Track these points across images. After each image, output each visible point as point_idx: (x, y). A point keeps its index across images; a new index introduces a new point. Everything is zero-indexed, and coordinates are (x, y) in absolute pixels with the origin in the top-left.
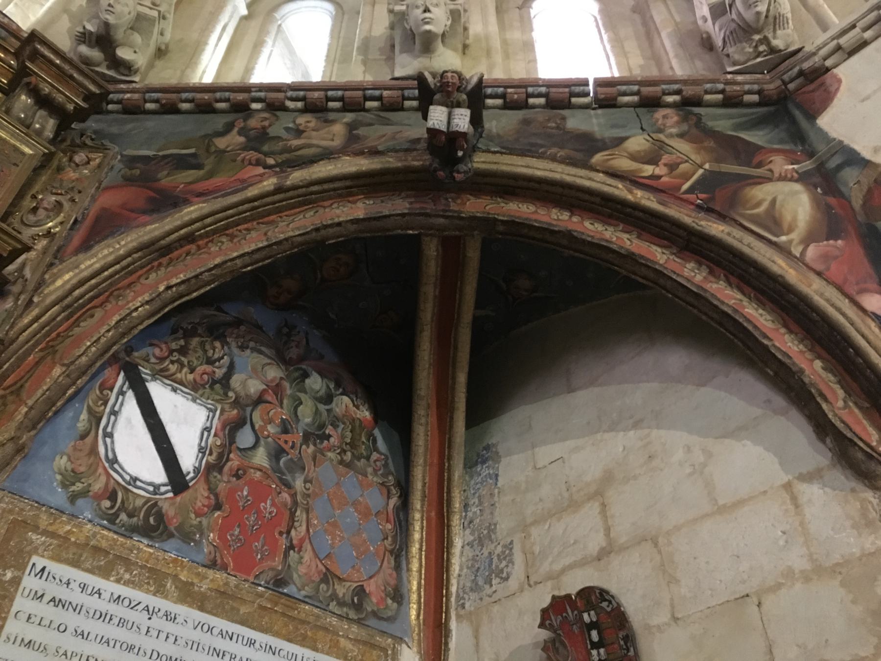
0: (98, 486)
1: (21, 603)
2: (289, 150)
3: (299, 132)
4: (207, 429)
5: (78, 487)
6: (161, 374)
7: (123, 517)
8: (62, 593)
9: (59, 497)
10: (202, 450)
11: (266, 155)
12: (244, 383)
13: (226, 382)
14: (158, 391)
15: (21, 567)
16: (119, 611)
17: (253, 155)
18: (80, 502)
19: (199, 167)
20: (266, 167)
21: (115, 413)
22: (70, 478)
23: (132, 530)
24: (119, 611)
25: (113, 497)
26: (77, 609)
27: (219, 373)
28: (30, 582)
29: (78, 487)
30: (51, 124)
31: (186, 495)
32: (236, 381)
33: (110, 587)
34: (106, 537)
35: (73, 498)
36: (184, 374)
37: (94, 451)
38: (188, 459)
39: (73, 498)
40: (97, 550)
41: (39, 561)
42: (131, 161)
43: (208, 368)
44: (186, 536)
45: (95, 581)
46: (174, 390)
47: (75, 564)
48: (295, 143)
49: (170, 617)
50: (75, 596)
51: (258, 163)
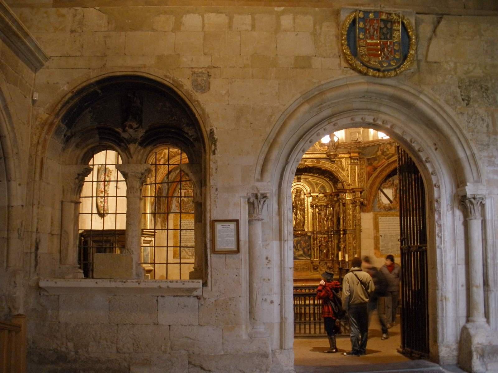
0: (382, 207)
1: (380, 223)
2: (387, 155)
3: (388, 149)
4: (393, 193)
5: (380, 208)
6: (384, 188)
7: (386, 209)
8: (383, 220)
9: (378, 210)
10: (393, 196)
11: (385, 156)
12: (396, 182)
13: (393, 184)
14: (385, 190)
15: (378, 219)
16: (390, 220)
17: (383, 157)
18: (381, 209)
19: (377, 160)
20: (386, 159)
21: (380, 196)
22: (379, 207)
23: (388, 210)
24: (390, 220)
25: (384, 207)
26: (385, 221)
27: (392, 182)
28: (379, 220)
29: (380, 208)
30: (357, 160)
31: (393, 203)
32: (395, 183)
33: (388, 218)
34: (385, 212)
35: (380, 209)
36: (387, 186)
37: (380, 203)
38: (391, 198)
39: (380, 209)
40: (385, 214)
41: (380, 218)
42: (368, 159)
43: (390, 183)
44: (394, 208)
45: (386, 218)
46: (386, 189)
47: (383, 216)
48: (388, 152)
49: (395, 219)
50: (385, 220)
51: (384, 159)
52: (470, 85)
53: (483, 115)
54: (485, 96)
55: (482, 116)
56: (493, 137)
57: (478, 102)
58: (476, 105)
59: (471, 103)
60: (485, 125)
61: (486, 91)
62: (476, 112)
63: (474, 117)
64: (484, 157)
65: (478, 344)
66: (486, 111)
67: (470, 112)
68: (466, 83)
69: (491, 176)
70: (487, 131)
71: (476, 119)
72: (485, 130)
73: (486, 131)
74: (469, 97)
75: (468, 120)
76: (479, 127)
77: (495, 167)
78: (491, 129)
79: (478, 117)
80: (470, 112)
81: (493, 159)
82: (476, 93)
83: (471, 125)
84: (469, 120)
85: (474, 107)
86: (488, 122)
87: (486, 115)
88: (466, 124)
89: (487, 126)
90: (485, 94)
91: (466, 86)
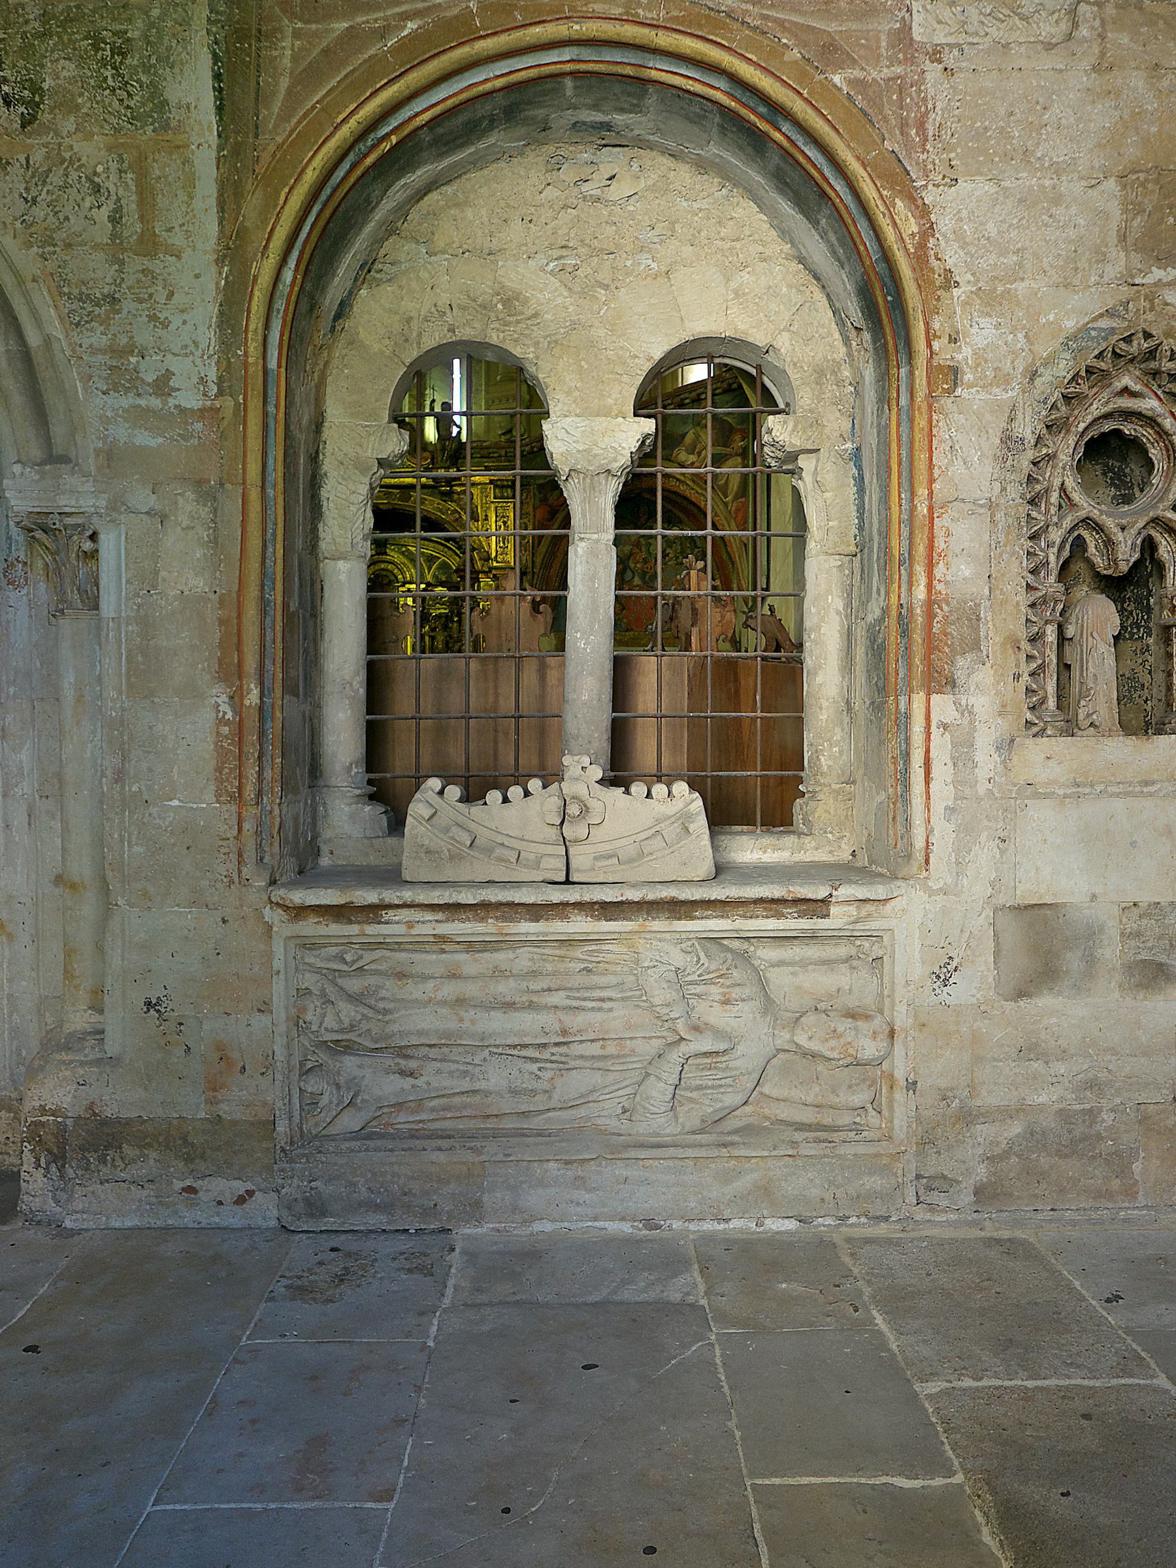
52: (44, 35)
53: (100, 169)
54: (110, 82)
55: (95, 174)
56: (134, 264)
57: (78, 107)
58: (69, 124)
59: (45, 117)
60: (105, 212)
61: (118, 59)
62: (67, 155)
63: (56, 179)
64: (93, 350)
65: (43, 1110)
66: (110, 149)
67: (38, 157)
68: (27, 22)
69: (121, 433)
70: (114, 236)
71: (64, 187)
72: (102, 231)
73: (106, 240)
74: (36, 89)
75: (27, 189)
76: (76, 223)
77: (139, 395)
78: (133, 226)
79: (74, 175)
80: (38, 157)
81: (133, 360)
82: (69, 69)
83: (39, 212)
84: (34, 192)
85: (57, 133)
86: (119, 200)
87: (114, 166)
88: (21, 206)
89: (116, 218)
90: (108, 73)
91: (24, 36)
